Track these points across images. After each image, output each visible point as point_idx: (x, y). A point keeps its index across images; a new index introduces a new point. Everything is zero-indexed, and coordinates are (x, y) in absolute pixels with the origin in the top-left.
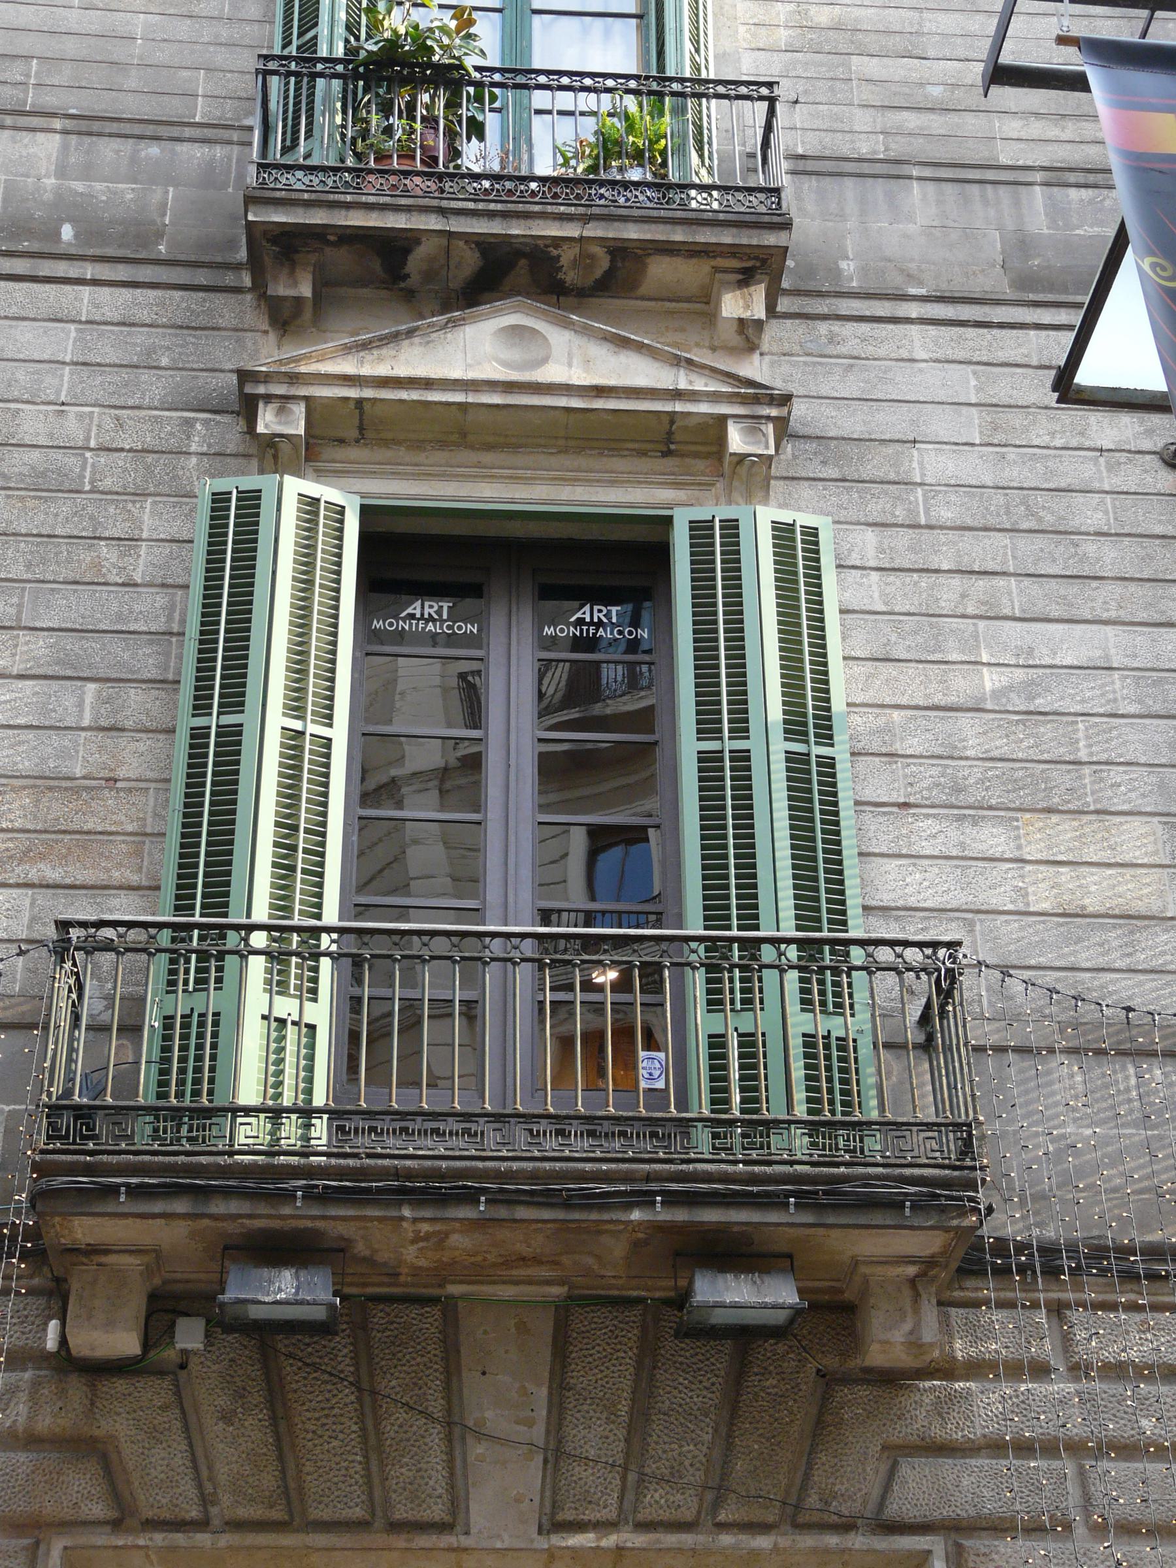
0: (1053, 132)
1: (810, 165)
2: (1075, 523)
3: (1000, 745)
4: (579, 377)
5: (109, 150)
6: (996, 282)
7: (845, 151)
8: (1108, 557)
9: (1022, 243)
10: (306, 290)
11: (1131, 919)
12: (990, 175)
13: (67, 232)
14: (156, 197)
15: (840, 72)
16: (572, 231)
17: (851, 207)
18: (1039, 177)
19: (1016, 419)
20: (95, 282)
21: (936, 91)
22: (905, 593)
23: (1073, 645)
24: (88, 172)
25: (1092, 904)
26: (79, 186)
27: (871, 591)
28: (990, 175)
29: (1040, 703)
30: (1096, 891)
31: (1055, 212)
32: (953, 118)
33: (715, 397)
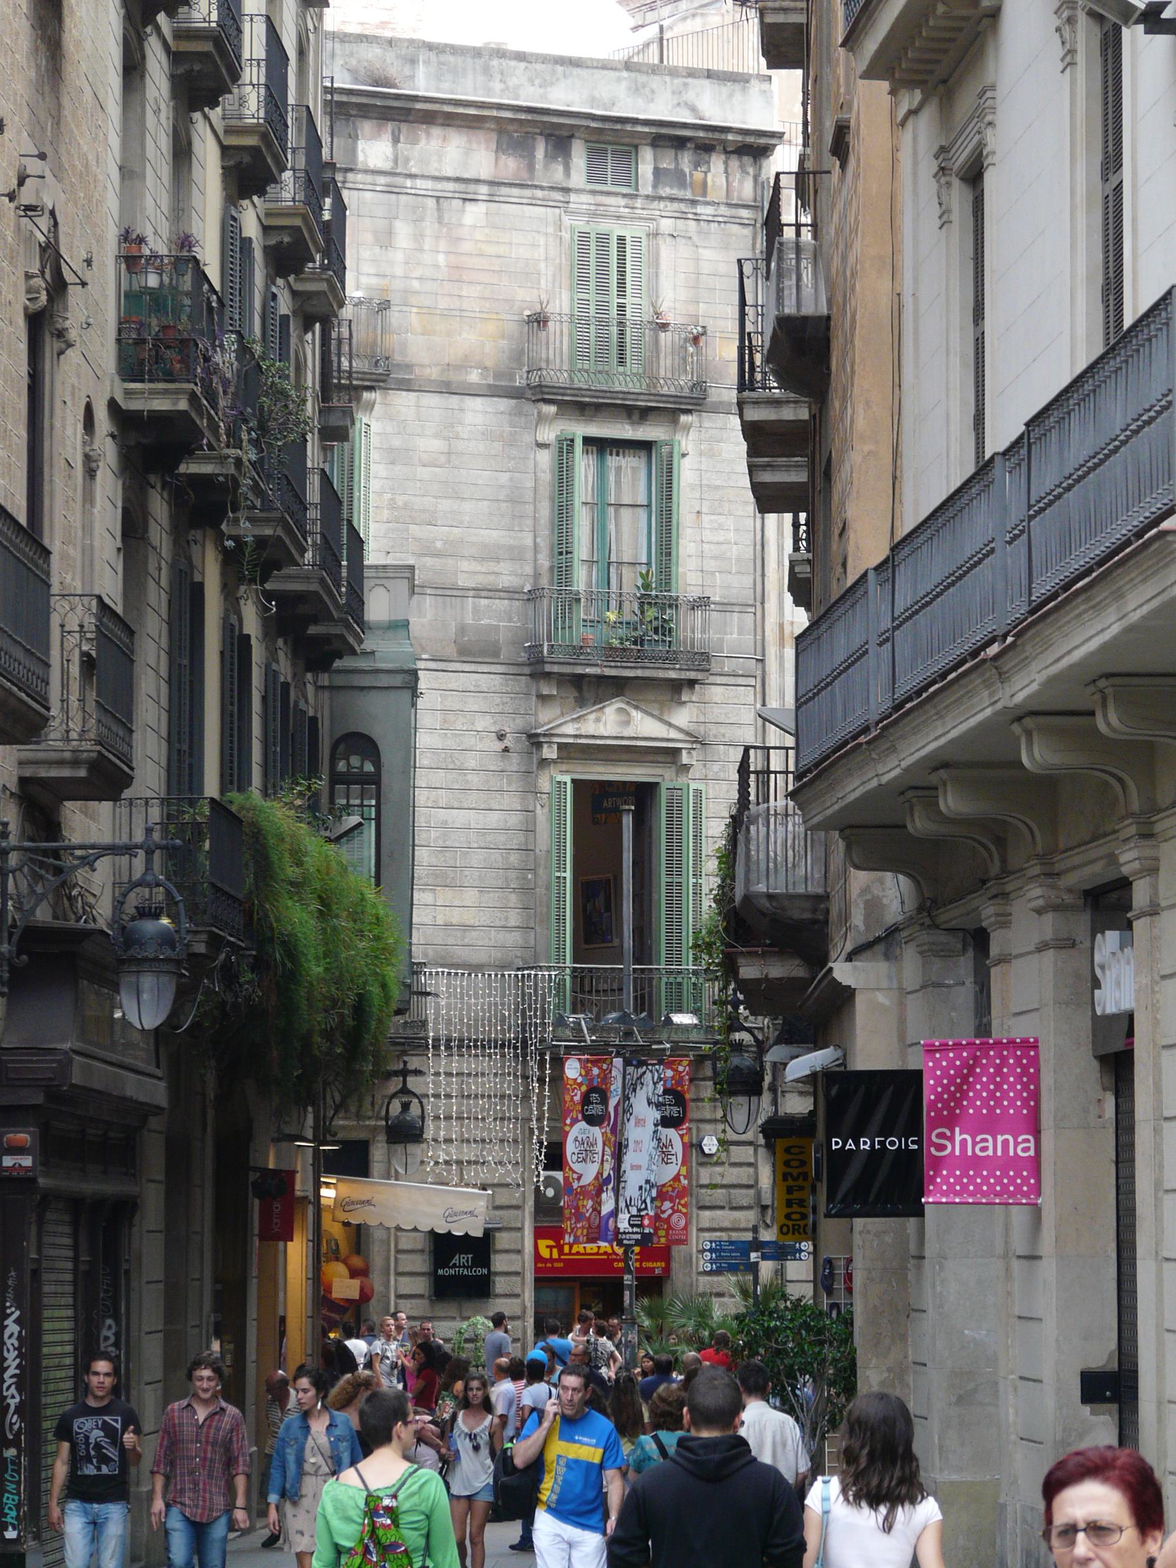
0: (479, 568)
2: (466, 765)
3: (434, 861)
6: (451, 651)
8: (474, 780)
9: (462, 629)
11: (466, 927)
12: (455, 593)
18: (471, 593)
19: (451, 717)
21: (439, 544)
23: (459, 817)
25: (454, 921)
28: (455, 593)
29: (448, 843)
30: (456, 916)
31: (476, 610)
32: (443, 560)
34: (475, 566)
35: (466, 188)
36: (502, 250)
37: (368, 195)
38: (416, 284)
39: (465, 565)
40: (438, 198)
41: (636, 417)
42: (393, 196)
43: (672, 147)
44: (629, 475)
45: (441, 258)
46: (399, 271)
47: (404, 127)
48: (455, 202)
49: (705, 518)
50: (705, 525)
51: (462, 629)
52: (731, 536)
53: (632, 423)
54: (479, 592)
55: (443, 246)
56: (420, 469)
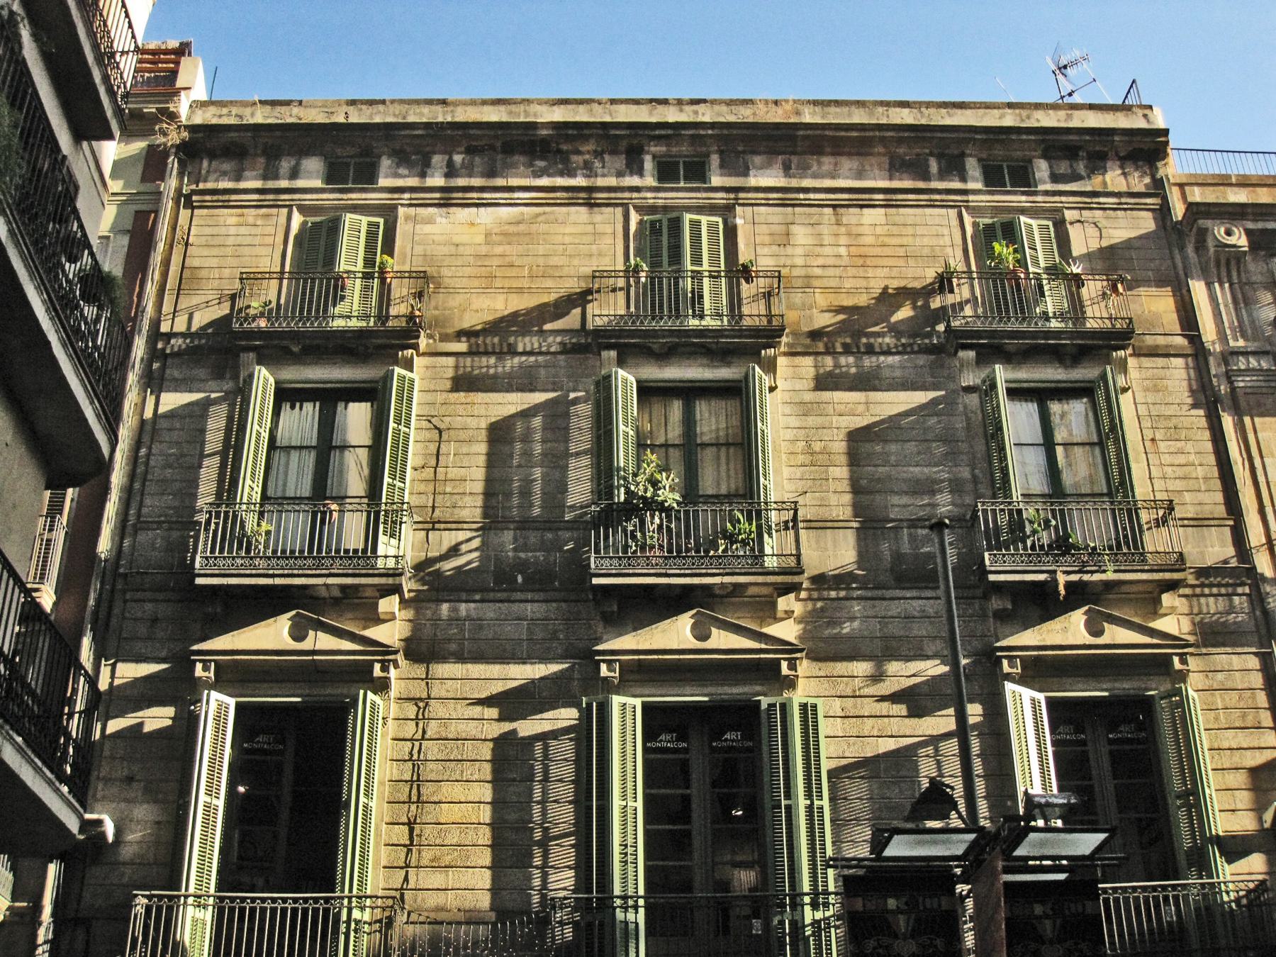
1: (813, 525)
4: (724, 646)
5: (533, 537)
7: (827, 516)
9: (898, 557)
10: (615, 608)
13: (520, 579)
14: (552, 559)
15: (823, 476)
16: (717, 580)
17: (830, 544)
20: (532, 601)
22: (852, 726)
24: (525, 548)
26: (522, 555)
27: (837, 727)
31: (913, 539)
33: (776, 651)
34: (905, 500)
35: (861, 199)
36: (905, 241)
37: (762, 209)
38: (818, 271)
39: (895, 500)
40: (834, 207)
41: (1068, 363)
42: (790, 209)
43: (1066, 158)
44: (1072, 418)
45: (843, 251)
46: (799, 261)
47: (795, 159)
48: (852, 210)
49: (1162, 446)
50: (1162, 450)
51: (898, 557)
52: (1192, 458)
53: (1066, 367)
54: (914, 523)
55: (843, 240)
56: (835, 419)
